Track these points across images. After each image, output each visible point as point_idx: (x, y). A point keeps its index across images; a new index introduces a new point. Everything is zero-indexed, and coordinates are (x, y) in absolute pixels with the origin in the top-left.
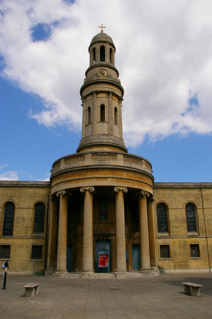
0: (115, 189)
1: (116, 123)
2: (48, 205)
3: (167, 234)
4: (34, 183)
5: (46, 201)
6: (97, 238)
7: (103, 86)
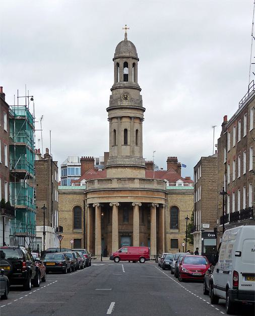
0: (133, 205)
1: (137, 144)
2: (84, 208)
3: (177, 231)
4: (72, 190)
5: (82, 205)
6: (122, 235)
7: (126, 112)
